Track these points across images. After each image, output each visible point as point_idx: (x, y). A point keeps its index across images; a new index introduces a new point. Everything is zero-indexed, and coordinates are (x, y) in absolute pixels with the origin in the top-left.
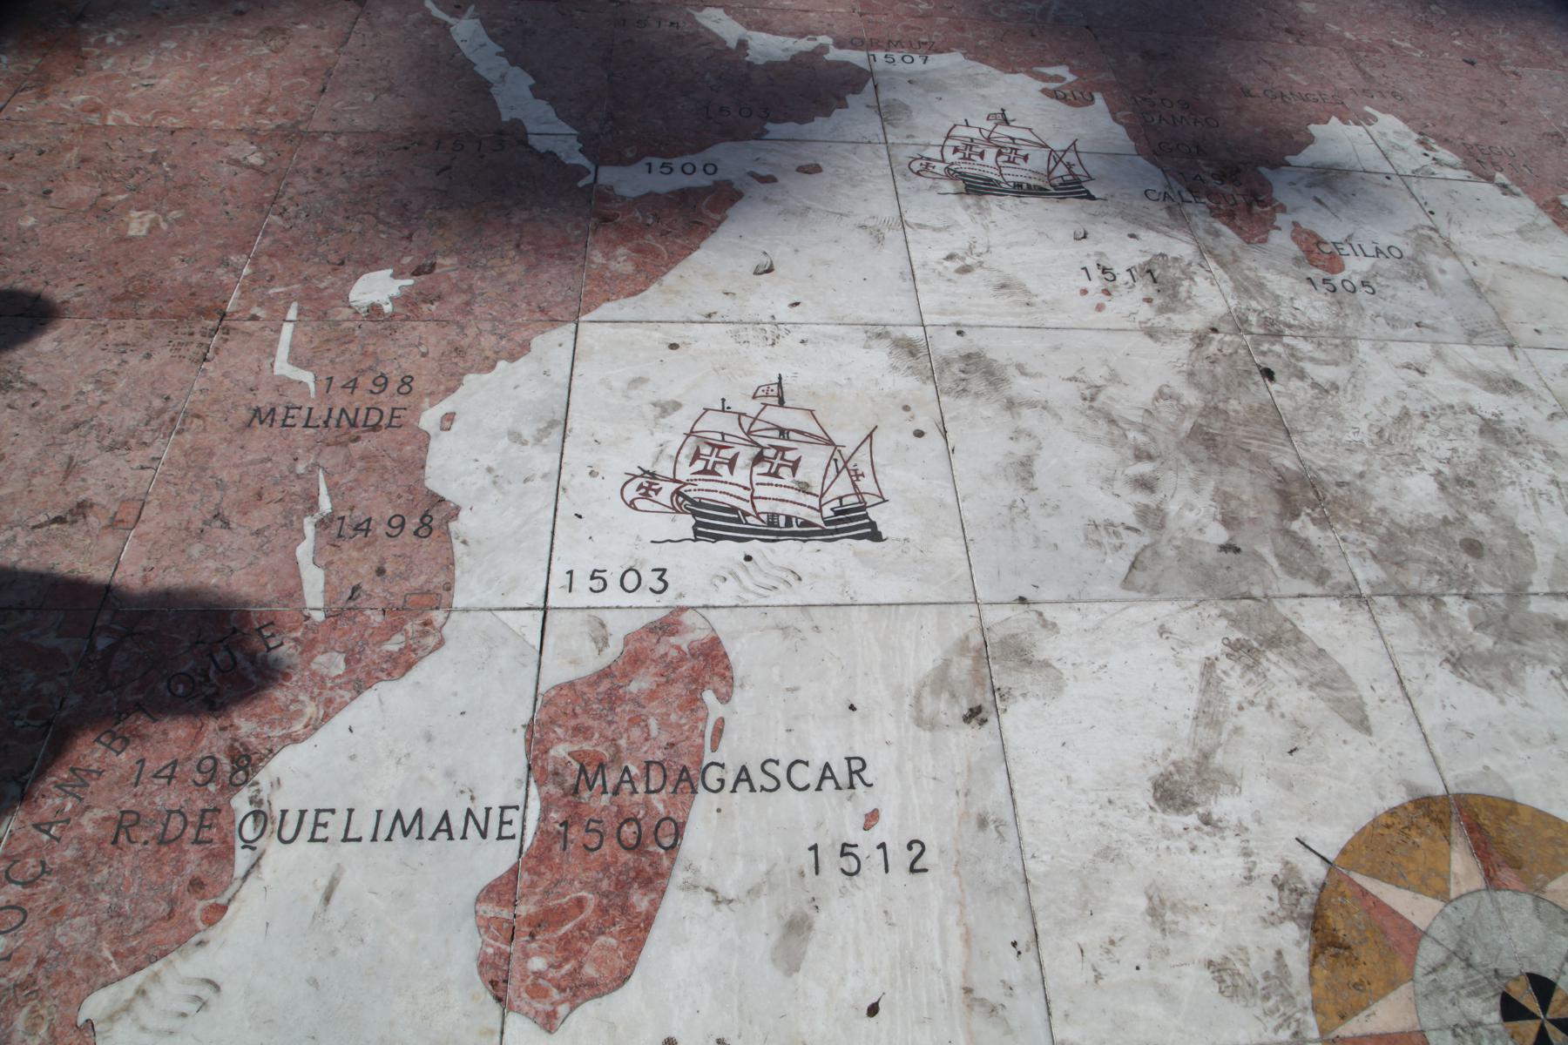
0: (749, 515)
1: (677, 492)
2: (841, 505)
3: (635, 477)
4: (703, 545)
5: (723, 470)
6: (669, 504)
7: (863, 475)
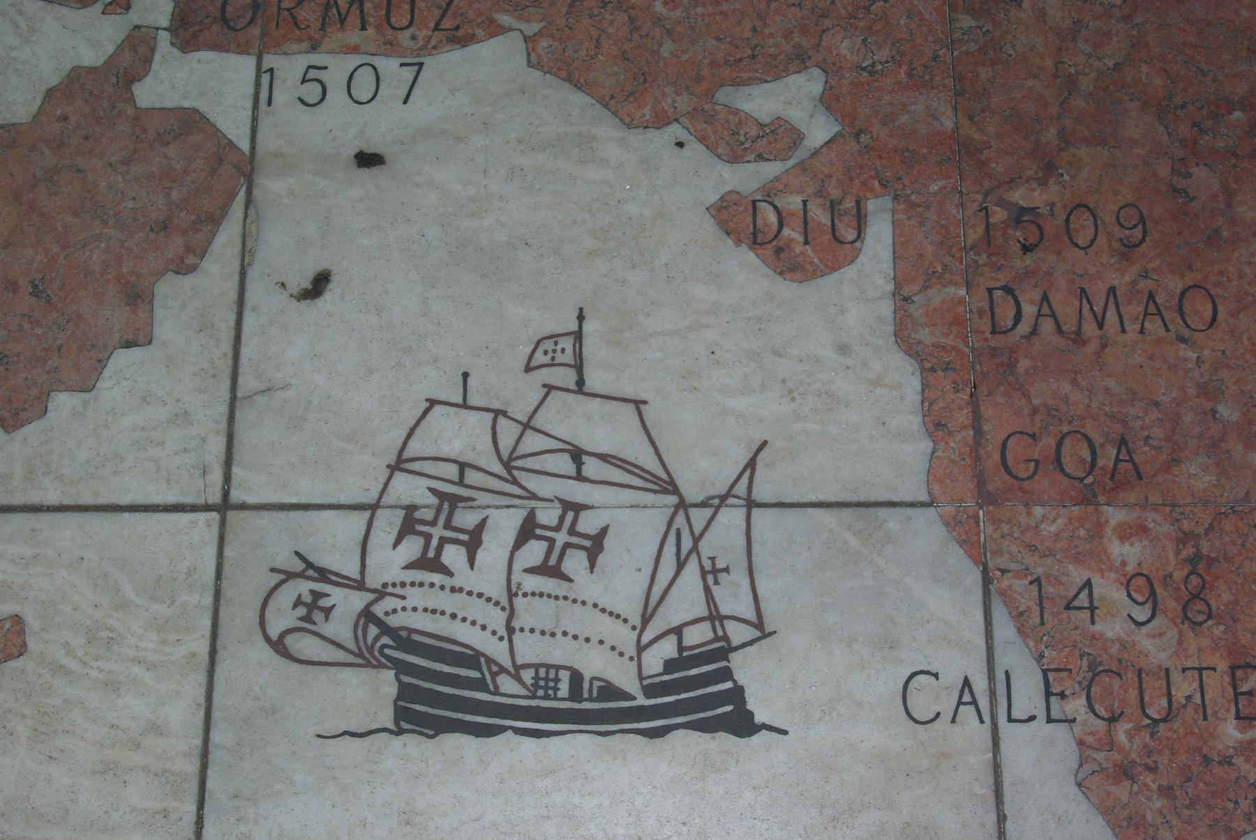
0: (503, 670)
1: (367, 615)
2: (681, 648)
3: (290, 575)
4: (412, 745)
5: (453, 556)
6: (352, 646)
7: (726, 570)
